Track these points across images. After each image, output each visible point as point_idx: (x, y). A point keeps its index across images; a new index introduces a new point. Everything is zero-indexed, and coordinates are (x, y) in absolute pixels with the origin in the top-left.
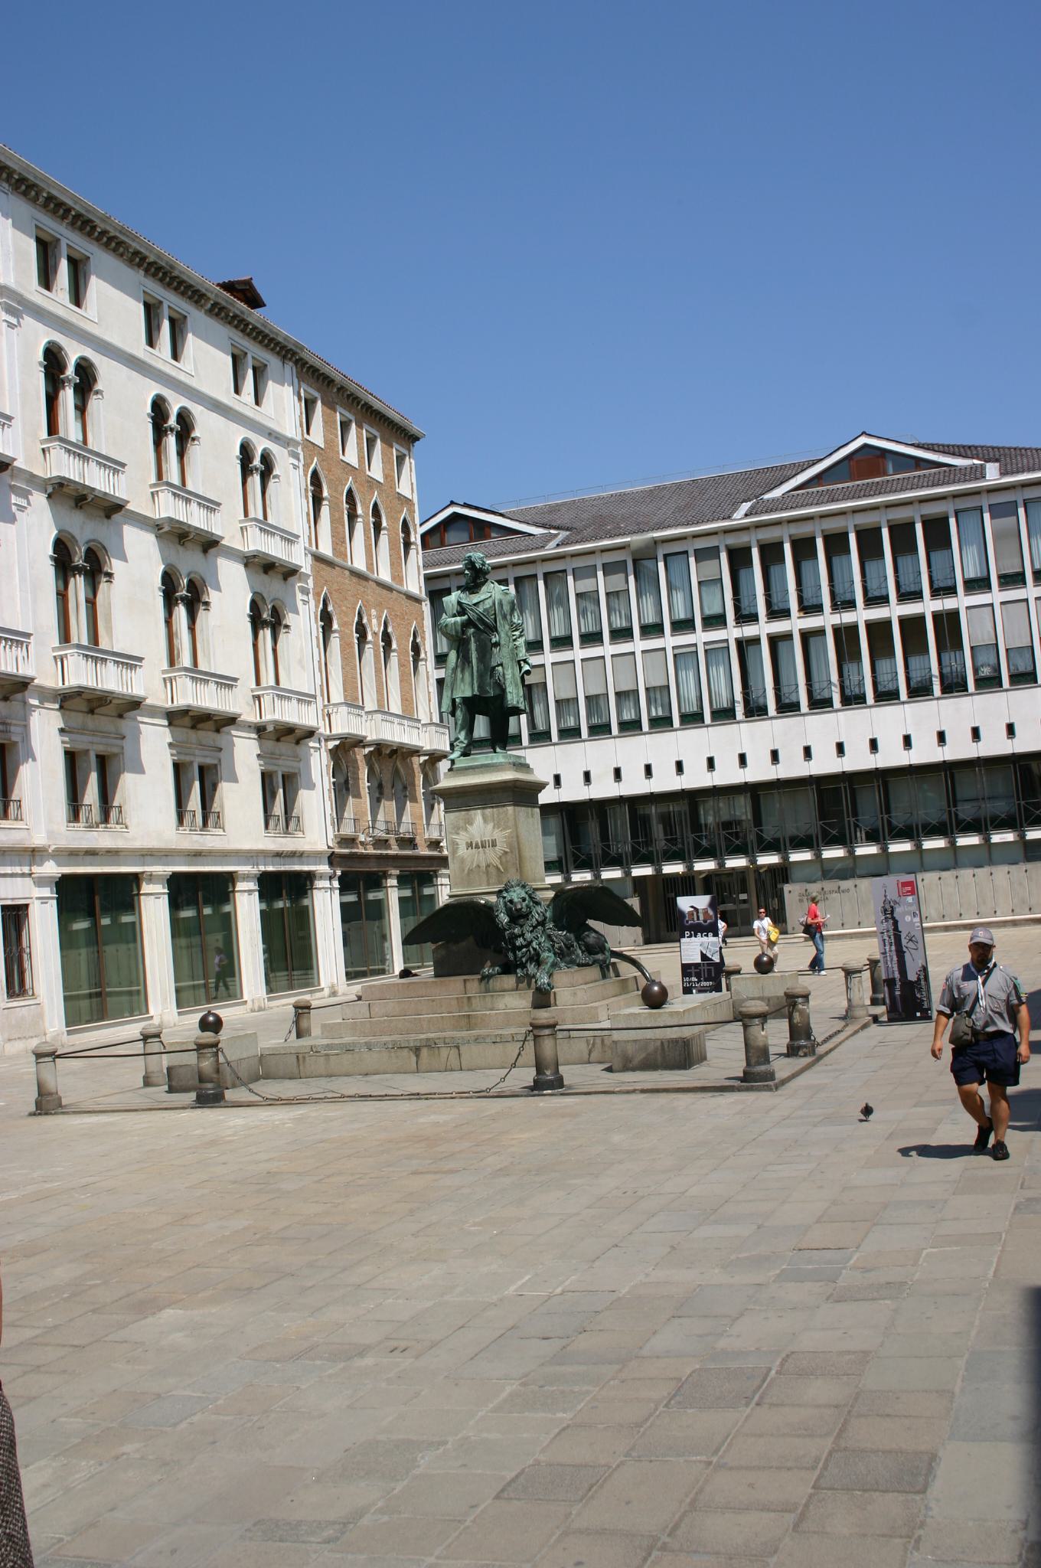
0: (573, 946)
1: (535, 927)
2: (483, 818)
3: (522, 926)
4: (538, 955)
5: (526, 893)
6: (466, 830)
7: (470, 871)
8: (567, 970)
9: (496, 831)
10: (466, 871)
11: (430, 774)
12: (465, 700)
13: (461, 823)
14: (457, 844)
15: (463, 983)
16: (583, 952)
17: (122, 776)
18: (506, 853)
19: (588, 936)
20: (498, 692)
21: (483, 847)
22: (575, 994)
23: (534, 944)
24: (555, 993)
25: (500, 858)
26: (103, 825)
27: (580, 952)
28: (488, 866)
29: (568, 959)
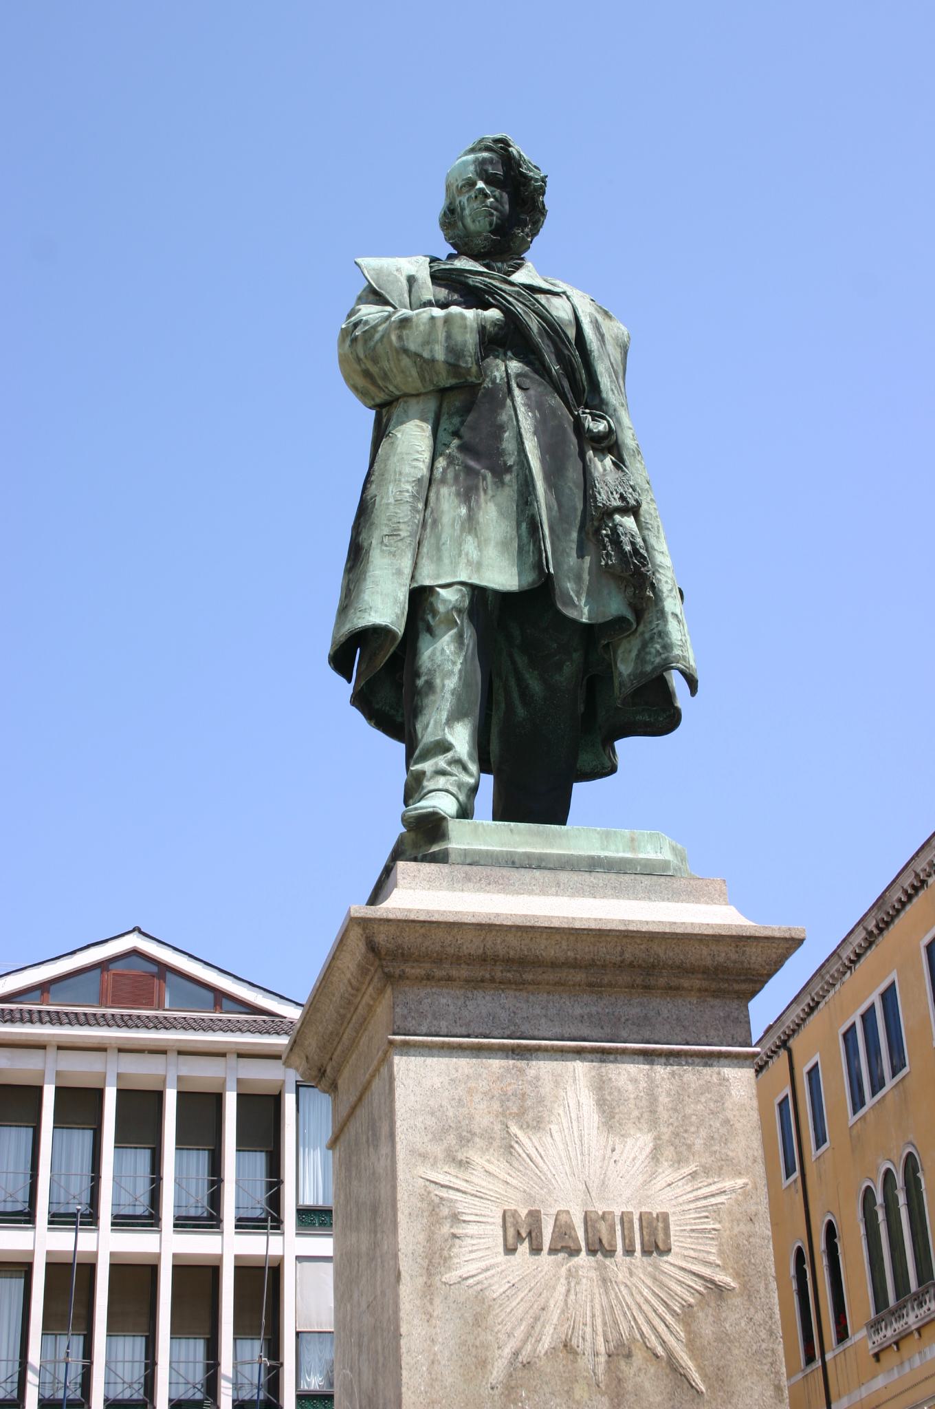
2: (601, 1103)
6: (508, 1148)
7: (522, 1367)
9: (667, 1174)
10: (498, 1371)
12: (478, 593)
13: (483, 1115)
14: (455, 1218)
18: (718, 1290)
20: (615, 606)
21: (598, 1248)
28: (620, 1352)
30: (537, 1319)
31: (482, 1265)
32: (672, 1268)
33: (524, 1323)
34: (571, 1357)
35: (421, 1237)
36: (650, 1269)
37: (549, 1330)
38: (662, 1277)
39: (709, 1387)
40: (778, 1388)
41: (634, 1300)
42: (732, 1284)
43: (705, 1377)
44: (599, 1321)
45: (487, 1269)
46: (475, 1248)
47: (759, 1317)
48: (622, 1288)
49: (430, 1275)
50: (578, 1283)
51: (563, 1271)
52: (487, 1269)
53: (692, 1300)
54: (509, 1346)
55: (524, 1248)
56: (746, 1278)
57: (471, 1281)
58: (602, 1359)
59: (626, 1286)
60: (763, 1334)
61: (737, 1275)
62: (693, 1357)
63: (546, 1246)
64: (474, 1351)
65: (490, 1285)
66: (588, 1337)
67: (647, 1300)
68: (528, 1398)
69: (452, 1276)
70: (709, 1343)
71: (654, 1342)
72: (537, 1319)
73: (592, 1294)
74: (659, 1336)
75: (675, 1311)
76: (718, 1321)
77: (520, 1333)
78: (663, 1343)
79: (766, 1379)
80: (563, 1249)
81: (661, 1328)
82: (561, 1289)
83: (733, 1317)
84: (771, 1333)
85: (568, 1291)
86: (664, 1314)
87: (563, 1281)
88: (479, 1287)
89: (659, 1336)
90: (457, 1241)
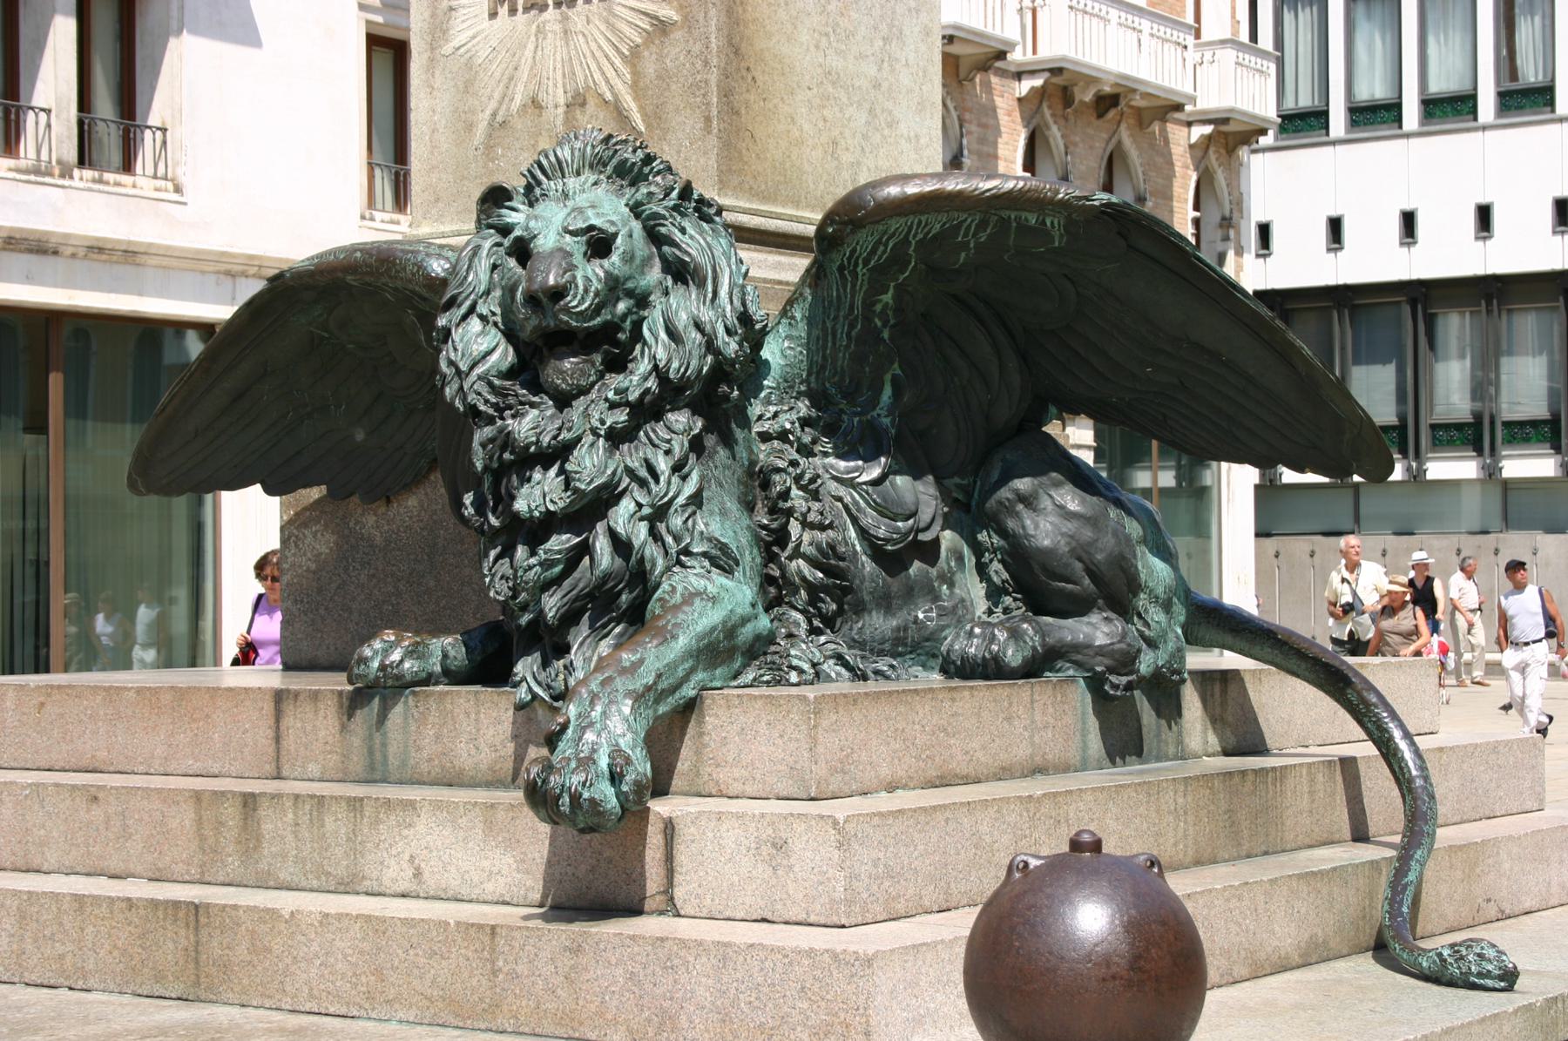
0: (929, 552)
1: (646, 411)
3: (563, 401)
4: (640, 579)
5: (636, 209)
7: (499, 126)
8: (843, 685)
11: (1220, 177)
15: (269, 707)
16: (994, 594)
17: (173, 43)
18: (662, 27)
19: (1028, 500)
22: (780, 846)
23: (622, 515)
24: (669, 828)
25: (635, 51)
26: (88, 174)
27: (976, 591)
28: (577, 101)
29: (879, 624)
30: (511, 79)
31: (470, 33)
32: (623, 10)
33: (502, 84)
34: (537, 111)
35: (427, 15)
36: (605, 14)
37: (520, 88)
38: (612, 20)
39: (648, 126)
40: (708, 119)
41: (589, 47)
42: (675, 18)
43: (645, 117)
44: (559, 73)
45: (474, 37)
46: (466, 17)
47: (697, 48)
48: (580, 37)
49: (433, 49)
50: (544, 38)
51: (534, 27)
52: (474, 37)
53: (639, 40)
54: (489, 108)
55: (503, 10)
56: (688, 10)
57: (462, 50)
58: (561, 110)
59: (584, 35)
60: (699, 65)
61: (681, 8)
62: (637, 98)
63: (520, 9)
64: (463, 115)
65: (477, 52)
66: (550, 91)
67: (600, 47)
68: (503, 156)
69: (447, 49)
70: (651, 82)
71: (604, 89)
72: (511, 79)
73: (556, 47)
74: (607, 81)
75: (623, 54)
76: (661, 58)
77: (497, 95)
78: (611, 88)
79: (698, 111)
80: (533, 6)
81: (610, 73)
82: (531, 46)
83: (674, 51)
84: (706, 63)
85: (537, 47)
86: (613, 58)
87: (533, 38)
88: (469, 55)
89: (607, 81)
90: (453, 12)
